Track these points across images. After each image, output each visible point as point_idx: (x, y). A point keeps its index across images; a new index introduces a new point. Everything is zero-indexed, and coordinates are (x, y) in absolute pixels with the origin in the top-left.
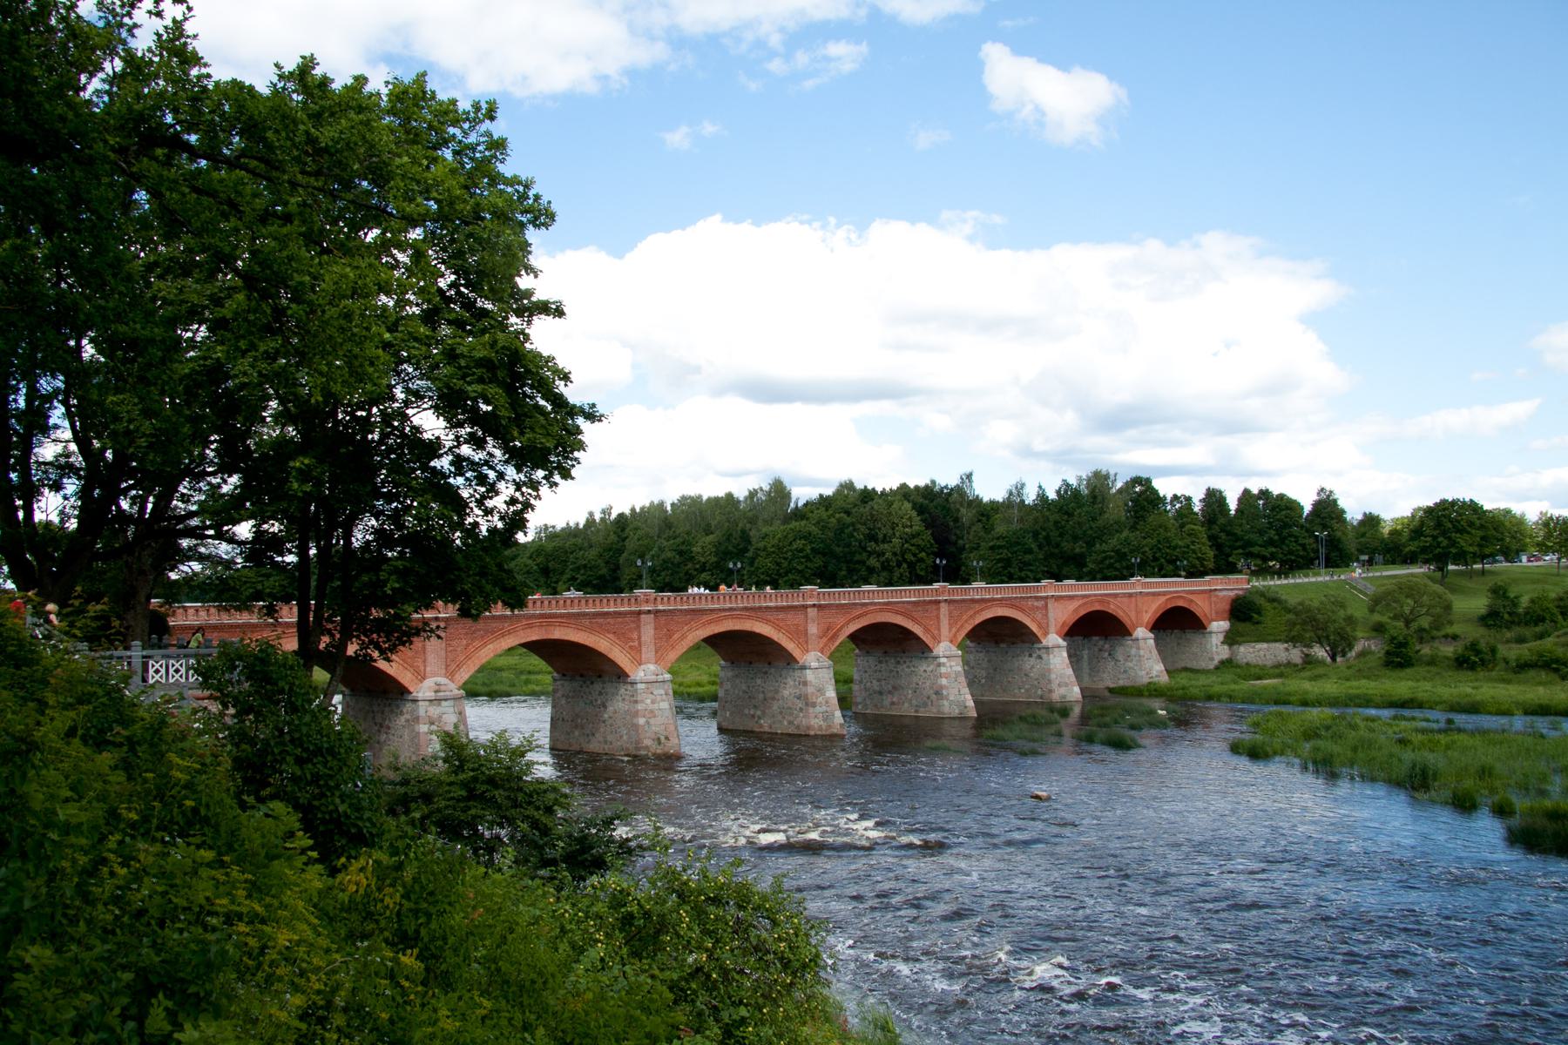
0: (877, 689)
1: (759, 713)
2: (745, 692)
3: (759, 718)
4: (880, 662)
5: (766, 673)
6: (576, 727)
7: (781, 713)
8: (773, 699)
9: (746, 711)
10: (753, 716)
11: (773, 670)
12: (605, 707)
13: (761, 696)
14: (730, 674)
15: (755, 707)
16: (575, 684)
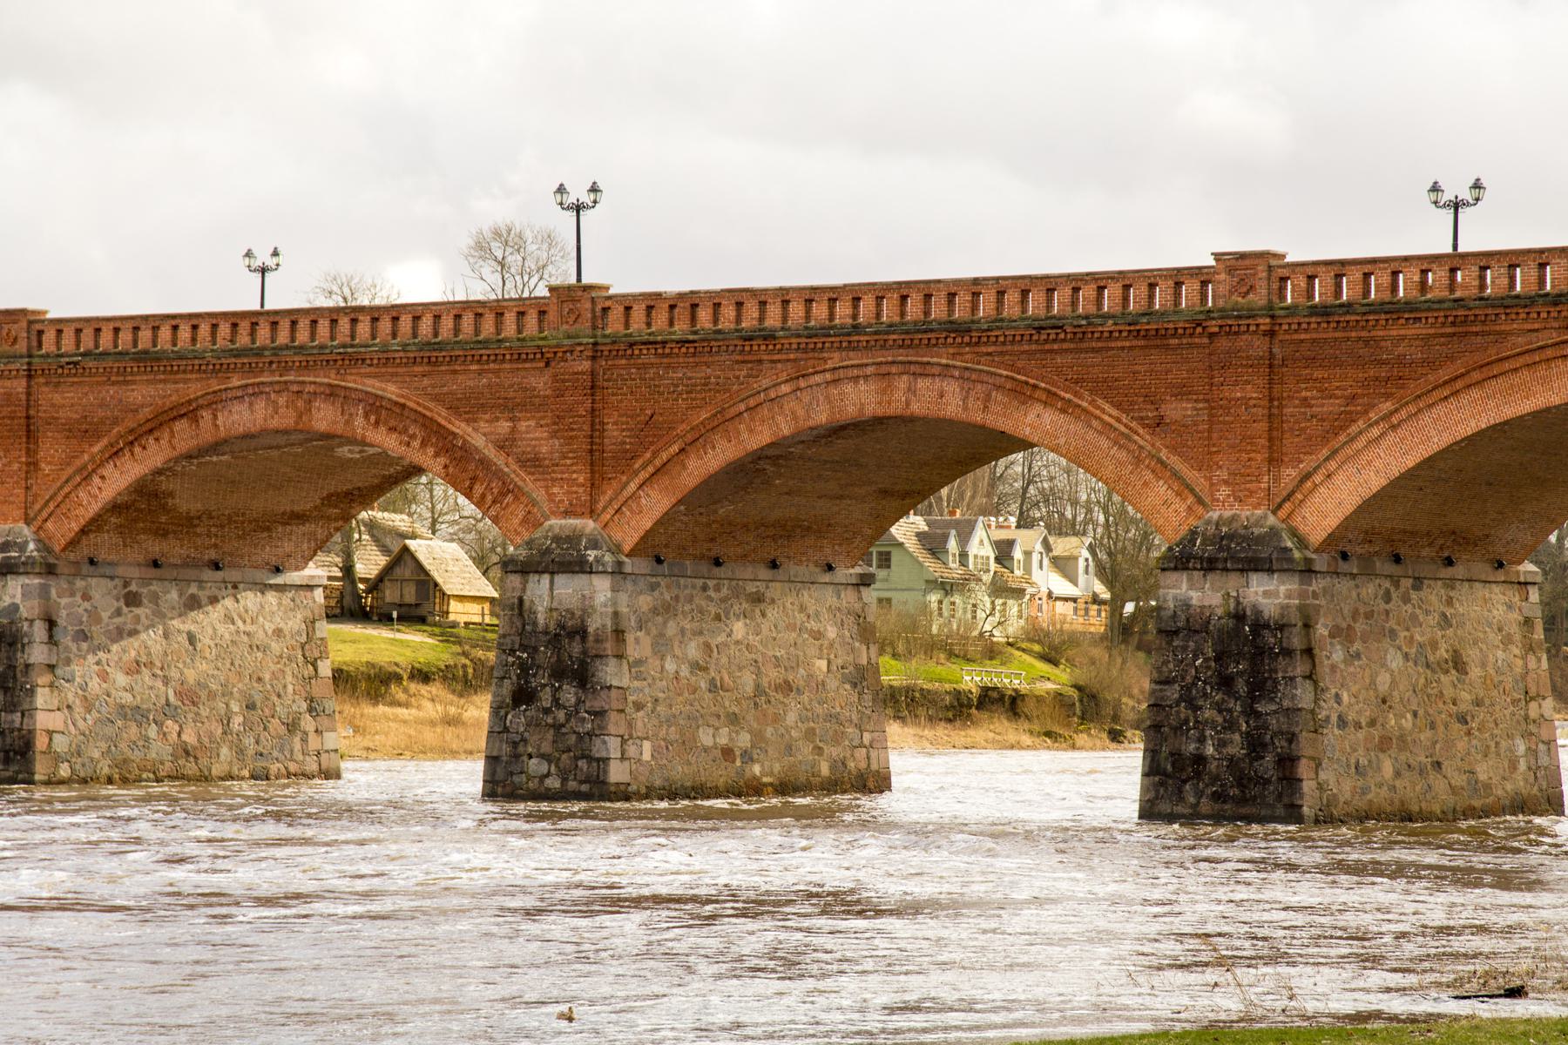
0: (127, 698)
1: (744, 740)
2: (696, 667)
3: (748, 757)
4: (132, 600)
5: (758, 599)
6: (1384, 744)
7: (810, 734)
8: (787, 687)
9: (705, 738)
10: (727, 753)
11: (775, 590)
12: (1458, 663)
13: (748, 680)
14: (645, 602)
15: (734, 720)
16: (1369, 589)
